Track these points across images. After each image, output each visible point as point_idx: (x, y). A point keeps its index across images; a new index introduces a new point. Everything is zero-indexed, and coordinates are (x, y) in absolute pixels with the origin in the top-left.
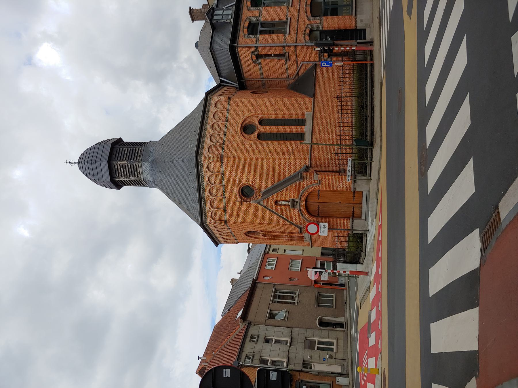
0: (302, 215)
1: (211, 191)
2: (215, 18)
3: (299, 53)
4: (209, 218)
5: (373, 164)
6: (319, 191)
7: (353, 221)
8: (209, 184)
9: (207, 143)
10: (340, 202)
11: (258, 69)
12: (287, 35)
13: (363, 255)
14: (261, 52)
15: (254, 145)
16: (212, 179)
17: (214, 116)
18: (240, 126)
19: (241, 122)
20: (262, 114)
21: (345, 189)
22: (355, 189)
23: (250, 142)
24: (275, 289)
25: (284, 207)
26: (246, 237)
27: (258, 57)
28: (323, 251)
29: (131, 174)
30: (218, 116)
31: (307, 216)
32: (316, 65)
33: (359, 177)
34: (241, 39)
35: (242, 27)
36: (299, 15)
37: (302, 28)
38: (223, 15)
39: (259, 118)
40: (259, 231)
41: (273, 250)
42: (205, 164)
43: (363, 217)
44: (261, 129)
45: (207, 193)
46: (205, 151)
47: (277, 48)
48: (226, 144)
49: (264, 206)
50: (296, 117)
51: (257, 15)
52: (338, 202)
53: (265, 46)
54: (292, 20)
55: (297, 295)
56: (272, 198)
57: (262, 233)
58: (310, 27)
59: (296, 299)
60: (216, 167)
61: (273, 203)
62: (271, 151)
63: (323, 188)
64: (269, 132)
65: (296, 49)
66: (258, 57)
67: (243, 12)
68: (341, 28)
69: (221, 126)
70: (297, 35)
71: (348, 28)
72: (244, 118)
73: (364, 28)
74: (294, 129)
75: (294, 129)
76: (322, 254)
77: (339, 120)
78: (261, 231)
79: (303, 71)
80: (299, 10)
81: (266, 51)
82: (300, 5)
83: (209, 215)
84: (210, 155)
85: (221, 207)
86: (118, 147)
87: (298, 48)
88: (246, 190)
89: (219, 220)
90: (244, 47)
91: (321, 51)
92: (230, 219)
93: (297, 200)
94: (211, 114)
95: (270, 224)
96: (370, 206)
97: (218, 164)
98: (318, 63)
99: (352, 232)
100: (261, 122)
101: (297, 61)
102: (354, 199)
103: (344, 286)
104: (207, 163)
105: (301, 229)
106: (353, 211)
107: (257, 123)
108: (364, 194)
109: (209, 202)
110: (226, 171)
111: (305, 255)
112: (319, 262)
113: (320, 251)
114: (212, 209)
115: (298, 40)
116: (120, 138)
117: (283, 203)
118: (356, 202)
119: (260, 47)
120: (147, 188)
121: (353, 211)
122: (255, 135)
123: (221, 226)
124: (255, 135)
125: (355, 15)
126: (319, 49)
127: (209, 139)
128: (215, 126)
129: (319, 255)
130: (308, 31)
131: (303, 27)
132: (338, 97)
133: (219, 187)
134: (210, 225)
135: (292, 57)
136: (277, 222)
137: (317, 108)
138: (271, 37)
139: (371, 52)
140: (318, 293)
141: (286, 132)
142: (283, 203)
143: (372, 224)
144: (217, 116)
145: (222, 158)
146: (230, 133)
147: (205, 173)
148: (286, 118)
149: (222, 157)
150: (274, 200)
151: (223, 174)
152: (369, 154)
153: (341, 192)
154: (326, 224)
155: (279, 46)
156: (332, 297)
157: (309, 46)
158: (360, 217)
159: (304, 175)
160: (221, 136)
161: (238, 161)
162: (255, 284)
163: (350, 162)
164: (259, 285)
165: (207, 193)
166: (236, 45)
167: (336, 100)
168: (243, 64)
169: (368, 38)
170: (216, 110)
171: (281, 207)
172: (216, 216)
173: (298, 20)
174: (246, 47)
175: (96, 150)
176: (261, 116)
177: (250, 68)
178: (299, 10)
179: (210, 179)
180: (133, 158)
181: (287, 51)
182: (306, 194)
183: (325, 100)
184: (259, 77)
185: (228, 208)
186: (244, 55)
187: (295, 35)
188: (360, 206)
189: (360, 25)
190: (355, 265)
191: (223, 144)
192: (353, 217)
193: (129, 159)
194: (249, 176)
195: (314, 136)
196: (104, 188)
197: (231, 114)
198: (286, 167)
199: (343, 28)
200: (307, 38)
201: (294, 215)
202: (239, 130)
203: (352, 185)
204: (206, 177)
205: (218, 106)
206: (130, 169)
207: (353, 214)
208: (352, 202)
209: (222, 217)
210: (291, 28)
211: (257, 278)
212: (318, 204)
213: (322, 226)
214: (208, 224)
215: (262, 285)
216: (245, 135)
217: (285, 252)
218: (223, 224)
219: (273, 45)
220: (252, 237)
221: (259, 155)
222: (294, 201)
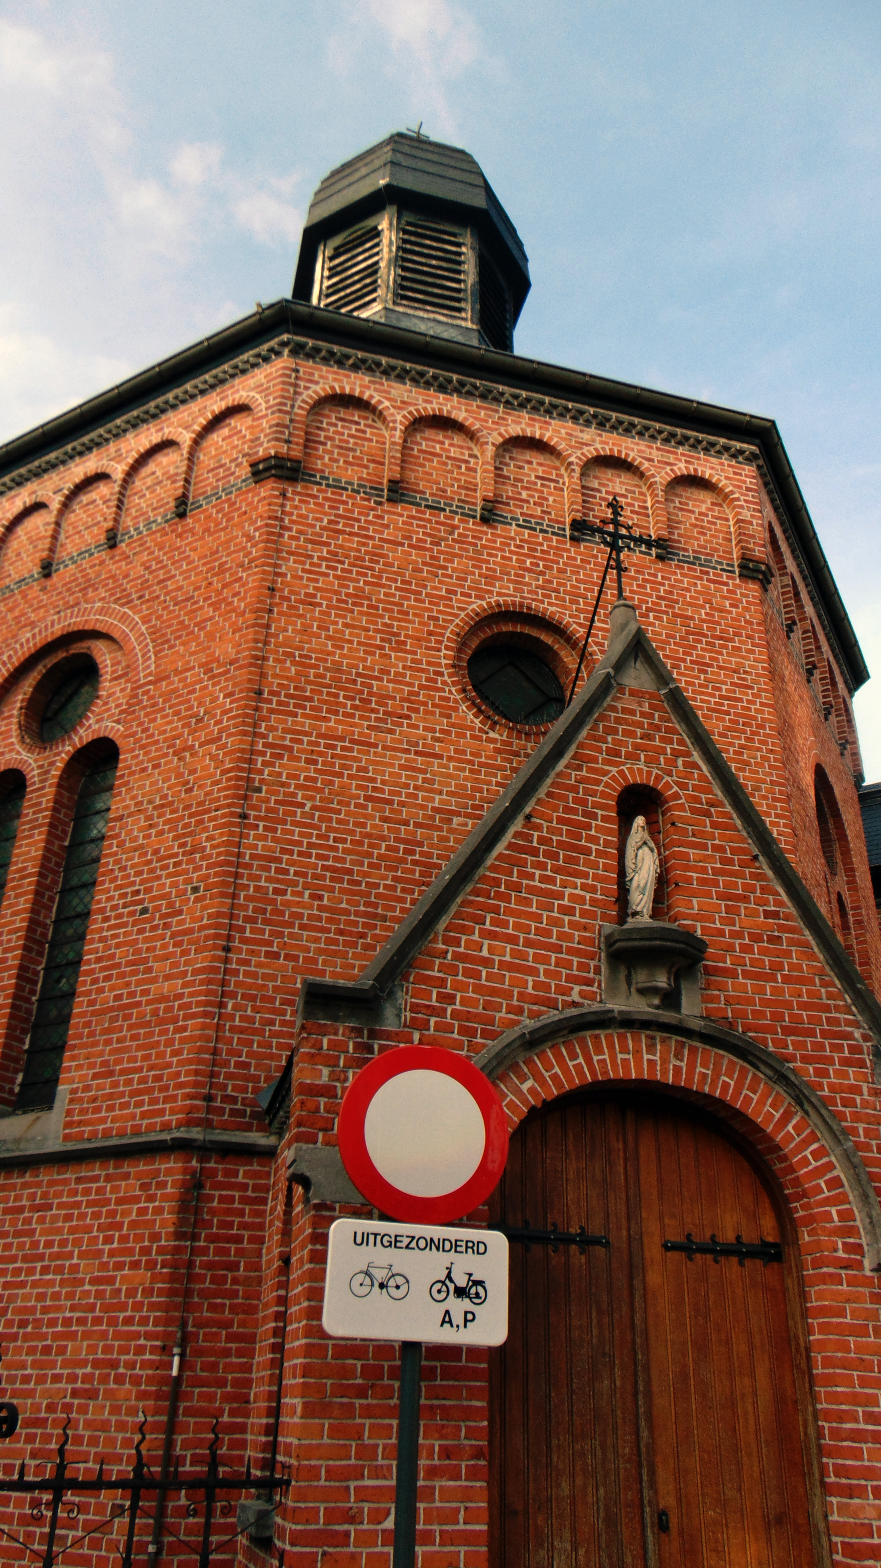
0: (533, 1041)
8: (590, 452)
40: (96, 724)
45: (521, 424)
52: (668, 1501)
89: (310, 442)
93: (691, 1007)
95: (245, 789)
109: (460, 415)
114: (399, 419)
117: (644, 868)
136: (257, 843)
142: (644, 868)
147: (655, 454)
150: (669, 785)
154: (491, 1327)
165: (521, 424)
172: (337, 428)
182: (762, 1104)
201: (531, 949)
206: (438, 281)
213: (464, 1266)
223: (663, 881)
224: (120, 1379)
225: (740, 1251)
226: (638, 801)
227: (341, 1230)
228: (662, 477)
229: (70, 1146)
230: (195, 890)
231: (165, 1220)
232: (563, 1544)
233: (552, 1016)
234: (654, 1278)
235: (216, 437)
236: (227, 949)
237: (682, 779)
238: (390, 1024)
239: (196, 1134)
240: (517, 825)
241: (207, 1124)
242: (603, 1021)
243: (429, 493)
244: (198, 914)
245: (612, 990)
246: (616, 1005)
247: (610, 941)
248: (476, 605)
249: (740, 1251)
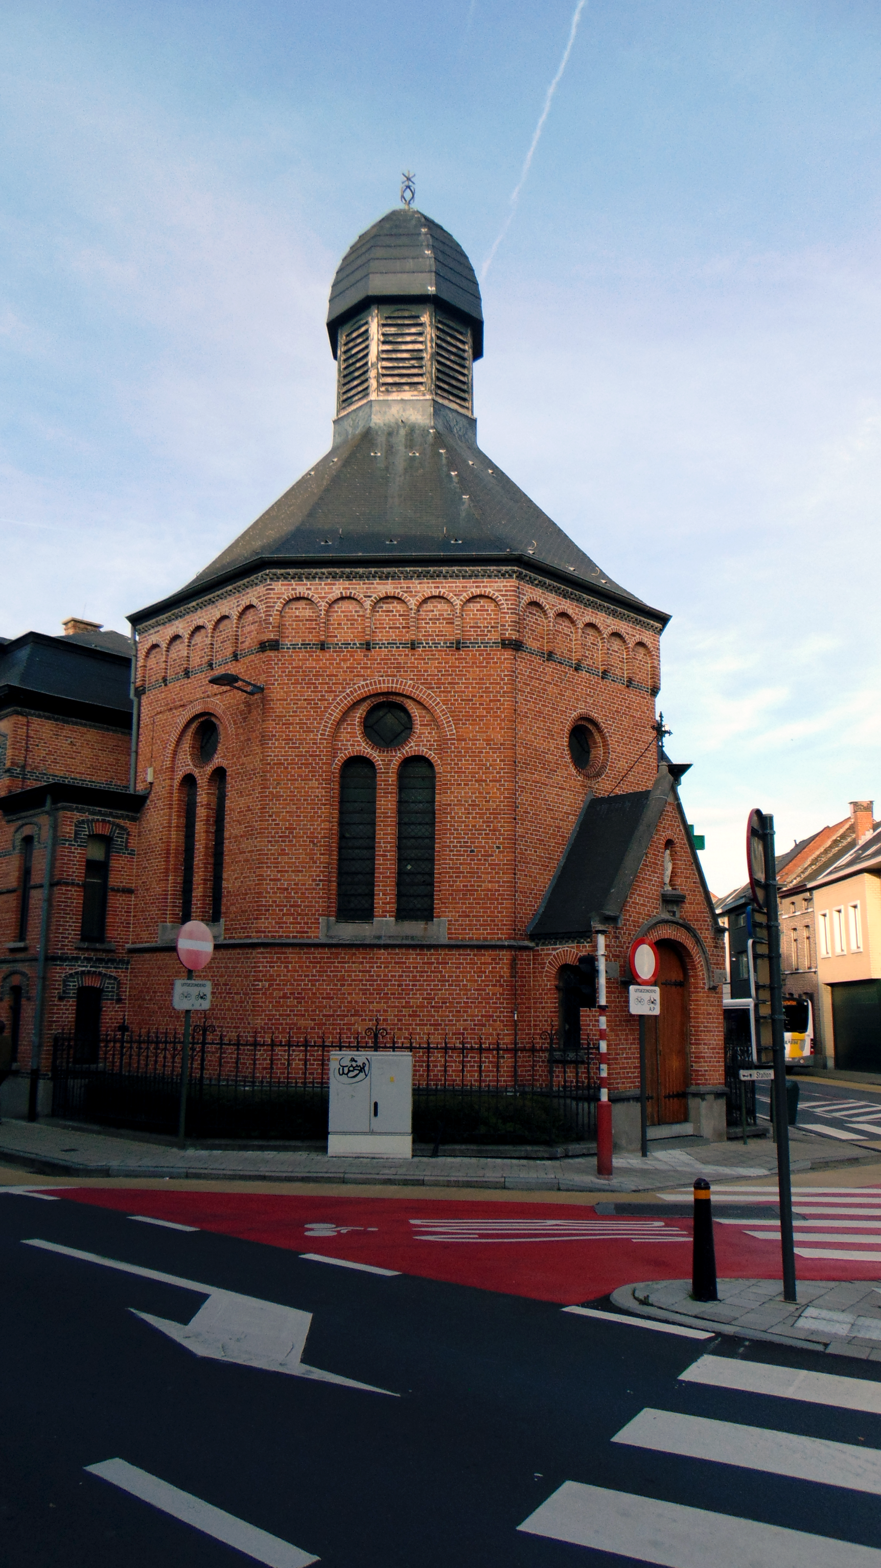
57: (387, 763)
109: (570, 612)
147: (630, 630)
182: (689, 943)
185: (550, 668)
218: (510, 634)
224: (494, 1021)
227: (632, 988)
229: (453, 942)
230: (498, 847)
231: (506, 971)
236: (515, 874)
238: (620, 925)
239: (512, 943)
241: (514, 939)
244: (500, 858)
248: (574, 714)
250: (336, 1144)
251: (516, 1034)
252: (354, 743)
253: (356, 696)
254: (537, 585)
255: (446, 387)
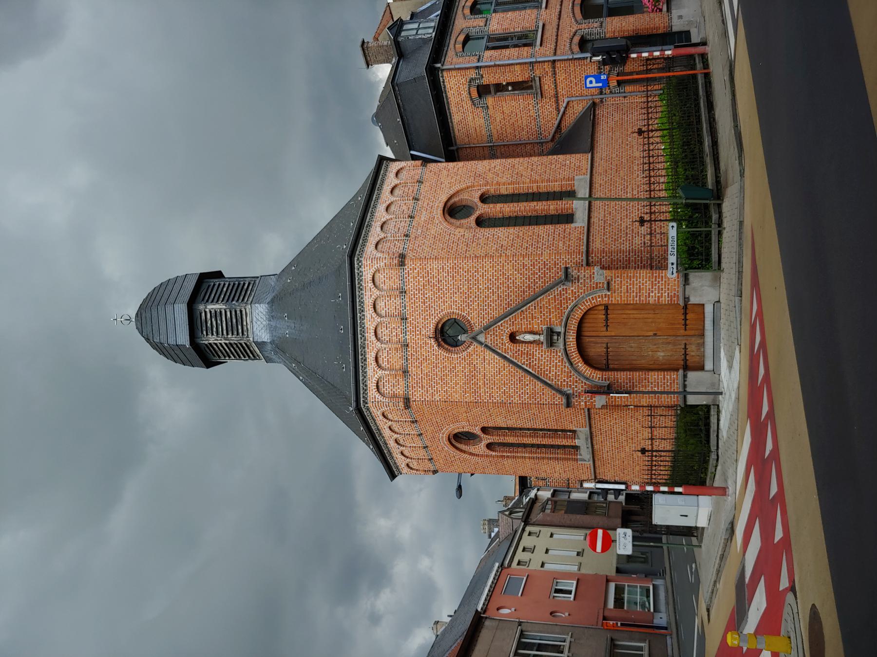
0: (571, 364)
1: (379, 332)
2: (403, 34)
3: (561, 76)
4: (372, 393)
5: (725, 234)
6: (606, 308)
7: (685, 376)
8: (374, 315)
9: (375, 233)
10: (655, 335)
11: (482, 121)
12: (538, 47)
13: (713, 456)
14: (489, 79)
15: (468, 235)
16: (380, 305)
17: (392, 192)
18: (442, 205)
19: (445, 199)
20: (487, 184)
21: (665, 300)
22: (686, 299)
23: (462, 230)
24: (522, 631)
25: (533, 348)
26: (451, 450)
27: (483, 91)
28: (621, 566)
29: (230, 328)
30: (401, 192)
31: (581, 366)
32: (594, 104)
33: (694, 276)
34: (450, 60)
35: (452, 42)
36: (559, 19)
37: (565, 36)
38: (418, 29)
39: (480, 193)
40: (477, 431)
41: (519, 563)
42: (366, 272)
43: (709, 366)
44: (483, 209)
46: (370, 248)
47: (517, 68)
48: (413, 236)
49: (486, 346)
50: (556, 187)
51: (482, 24)
52: (651, 333)
53: (495, 66)
54: (547, 27)
55: (567, 644)
56: (506, 328)
57: (487, 439)
58: (580, 33)
59: (566, 651)
60: (389, 279)
61: (506, 339)
62: (505, 243)
63: (615, 299)
64: (501, 215)
65: (554, 68)
66: (483, 91)
67: (456, 22)
68: (641, 33)
69: (405, 208)
70: (556, 46)
71: (655, 32)
72: (451, 192)
73: (686, 29)
74: (552, 207)
75: (552, 207)
76: (618, 571)
77: (646, 188)
78: (484, 430)
79: (570, 120)
80: (560, 12)
81: (497, 76)
82: (561, 5)
83: (371, 385)
84: (379, 255)
85: (398, 367)
86: (212, 282)
87: (558, 64)
88: (450, 332)
89: (394, 396)
90: (455, 69)
91: (604, 63)
92: (416, 395)
93: (559, 329)
94: (387, 188)
96: (723, 333)
97: (394, 272)
98: (597, 99)
99: (685, 397)
100: (484, 199)
101: (556, 96)
102: (686, 325)
103: (666, 628)
104: (372, 270)
105: (568, 397)
106: (686, 354)
107: (477, 200)
108: (709, 309)
109: (373, 355)
110: (409, 287)
111: (583, 571)
112: (612, 586)
113: (615, 566)
115: (558, 52)
116: (220, 272)
117: (529, 337)
118: (692, 332)
119: (486, 67)
120: (260, 365)
121: (686, 354)
122: (473, 219)
123: (397, 414)
124: (473, 219)
125: (668, 11)
126: (599, 58)
127: (379, 229)
128: (392, 208)
129: (612, 572)
130: (576, 39)
131: (567, 35)
132: (640, 132)
133: (395, 324)
134: (372, 409)
135: (546, 87)
137: (598, 169)
138: (506, 52)
139: (704, 57)
140: (612, 640)
141: (535, 214)
142: (529, 337)
143: (730, 367)
144: (397, 192)
145: (402, 259)
146: (423, 217)
147: (368, 293)
148: (535, 190)
149: (402, 257)
150: (508, 331)
151: (403, 292)
152: (715, 217)
153: (657, 307)
155: (520, 64)
156: (640, 649)
157: (579, 59)
158: (701, 368)
159: (574, 273)
160: (403, 224)
161: (435, 265)
162: (478, 622)
163: (673, 233)
164: (487, 623)
165: (370, 336)
166: (439, 65)
167: (636, 135)
168: (453, 109)
169: (695, 39)
170: (396, 181)
171: (522, 348)
172: (387, 389)
173: (558, 25)
174: (459, 69)
175: (170, 287)
176: (484, 189)
177: (466, 116)
178: (560, 12)
179: (378, 307)
180: (236, 299)
181: (538, 73)
182: (578, 314)
183: (614, 156)
184: (485, 139)
185: (412, 370)
186: (456, 88)
187: (553, 47)
188: (701, 341)
189: (677, 26)
190: (695, 497)
191: (407, 236)
192: (686, 368)
193: (228, 300)
194: (456, 298)
195: (594, 214)
196: (180, 366)
197: (424, 188)
198: (534, 274)
199: (645, 33)
200: (576, 48)
201: (552, 363)
202: (440, 211)
203: (681, 289)
204: (368, 301)
205: (401, 175)
207: (685, 360)
208: (682, 332)
209: (400, 390)
210: (545, 37)
211: (485, 610)
212: (606, 340)
214: (370, 405)
215: (494, 624)
216: (453, 220)
217: (543, 565)
218: (401, 405)
219: (511, 62)
220: (464, 452)
221: (480, 252)
222: (551, 332)
223: (532, 332)
225: (607, 314)
226: (513, 338)
228: (377, 293)
232: (659, 354)
233: (565, 360)
234: (613, 334)
235: (390, 416)
237: (506, 328)
238: (571, 392)
240: (524, 366)
242: (565, 349)
243: (401, 362)
245: (558, 347)
246: (562, 346)
247: (548, 347)
248: (436, 347)
249: (607, 314)
250: (702, 522)
251: (643, 406)
252: (480, 448)
253: (454, 449)
254: (366, 386)
255: (240, 327)
